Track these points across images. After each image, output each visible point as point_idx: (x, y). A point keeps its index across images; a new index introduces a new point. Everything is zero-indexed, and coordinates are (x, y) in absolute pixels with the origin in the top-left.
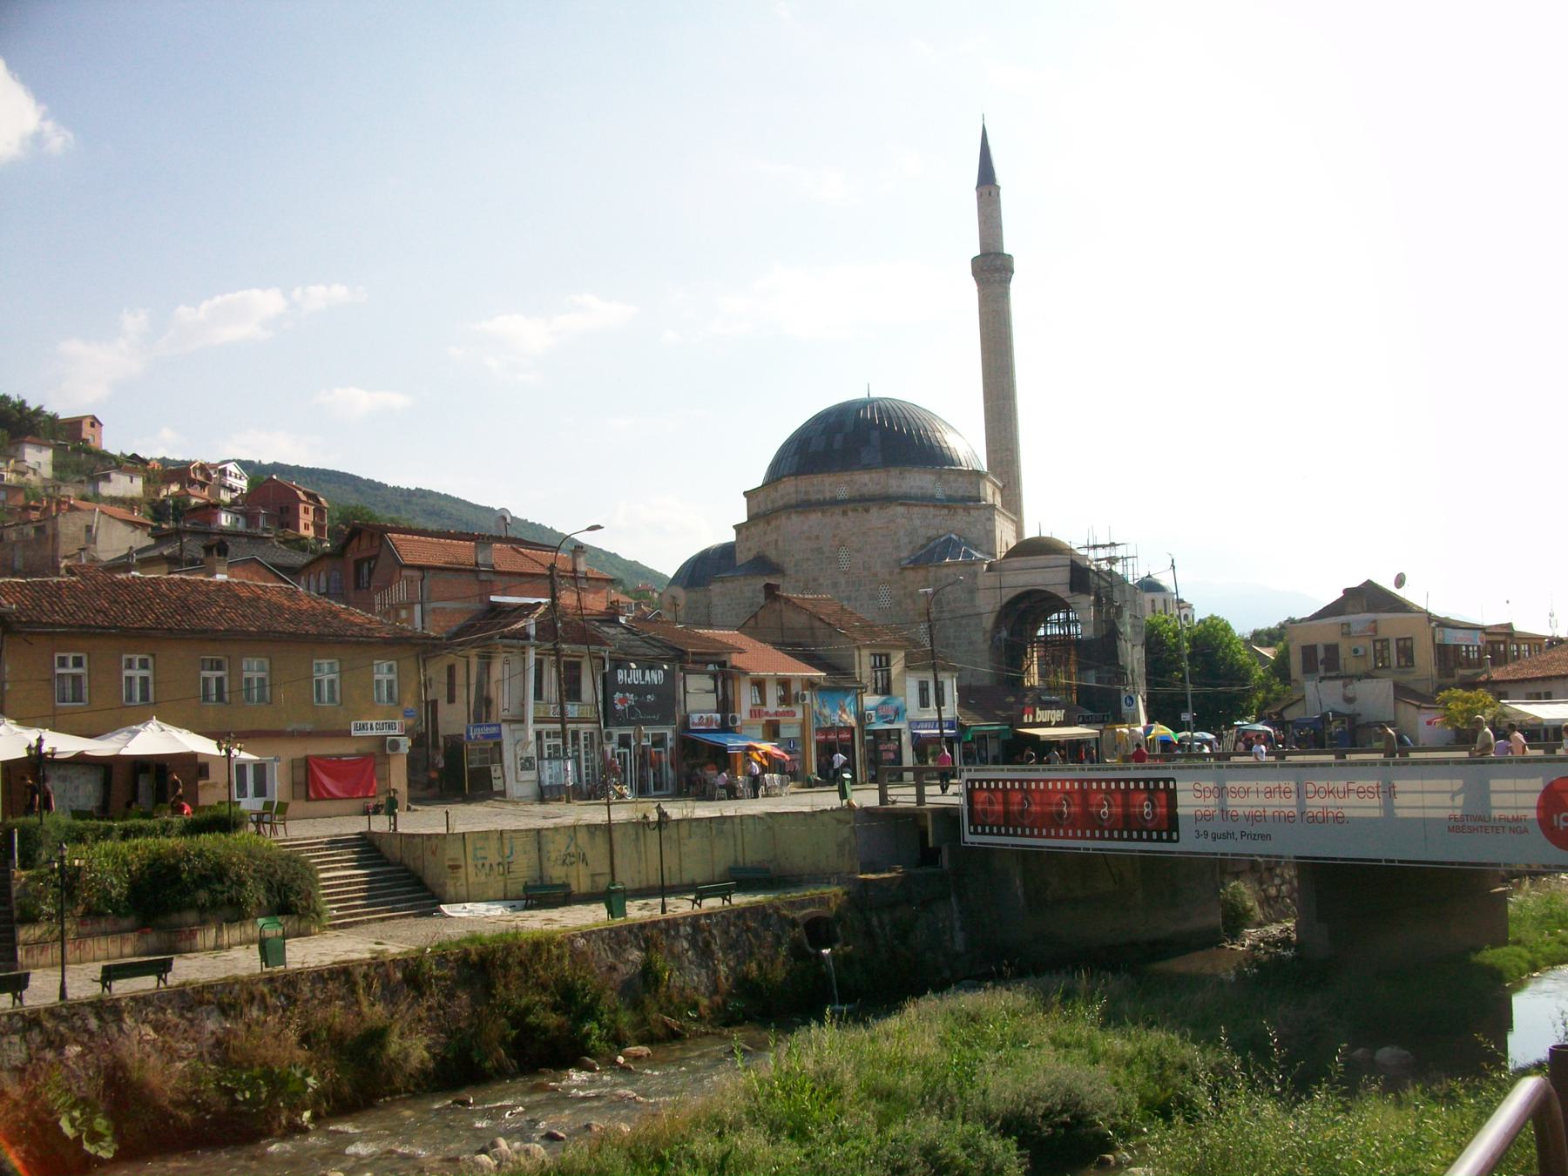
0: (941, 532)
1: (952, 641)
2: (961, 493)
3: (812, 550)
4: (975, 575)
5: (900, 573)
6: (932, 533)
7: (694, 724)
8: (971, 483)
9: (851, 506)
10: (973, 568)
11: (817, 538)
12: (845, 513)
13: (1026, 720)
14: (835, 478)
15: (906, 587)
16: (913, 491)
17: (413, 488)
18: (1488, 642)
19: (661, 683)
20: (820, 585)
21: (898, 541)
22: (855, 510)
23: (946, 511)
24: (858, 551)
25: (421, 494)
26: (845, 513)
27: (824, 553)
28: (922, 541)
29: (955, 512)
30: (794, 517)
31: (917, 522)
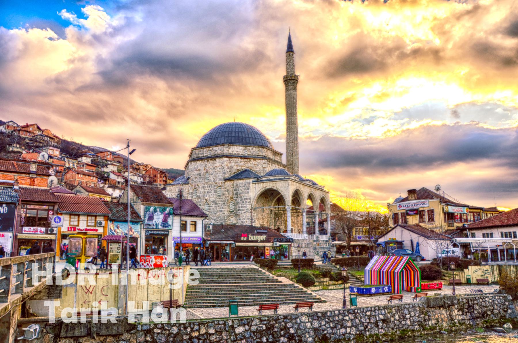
0: (243, 168)
1: (240, 208)
2: (254, 154)
3: (197, 175)
4: (249, 183)
5: (225, 183)
6: (239, 168)
7: (25, 231)
8: (259, 150)
11: (199, 170)
12: (208, 161)
13: (242, 238)
14: (207, 149)
16: (233, 153)
18: (470, 212)
19: (5, 212)
22: (211, 160)
23: (246, 160)
24: (212, 175)
26: (208, 161)
27: (201, 175)
28: (234, 171)
30: (192, 163)
31: (233, 164)
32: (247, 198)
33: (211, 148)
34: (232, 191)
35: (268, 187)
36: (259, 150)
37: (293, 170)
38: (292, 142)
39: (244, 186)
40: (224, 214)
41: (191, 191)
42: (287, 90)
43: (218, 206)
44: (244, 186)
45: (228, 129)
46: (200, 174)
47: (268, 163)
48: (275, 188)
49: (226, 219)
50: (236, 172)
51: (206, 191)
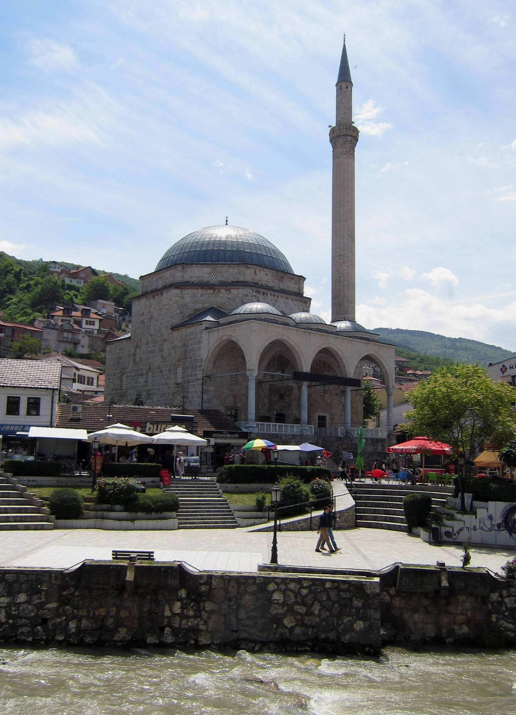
0: (207, 305)
2: (231, 279)
5: (172, 333)
6: (199, 306)
9: (156, 293)
10: (201, 326)
11: (143, 314)
12: (154, 296)
15: (172, 343)
16: (192, 280)
17: (457, 338)
20: (142, 343)
21: (173, 313)
22: (158, 294)
23: (211, 291)
24: (157, 321)
25: (461, 340)
27: (144, 323)
29: (220, 292)
32: (197, 359)
33: (161, 275)
34: (181, 347)
35: (224, 338)
36: (239, 272)
37: (340, 307)
38: (340, 255)
39: (195, 338)
40: (169, 388)
41: (132, 351)
42: (335, 157)
43: (163, 375)
44: (195, 338)
45: (194, 238)
46: (143, 321)
47: (254, 294)
48: (234, 339)
49: (171, 397)
50: (192, 315)
51: (150, 349)
